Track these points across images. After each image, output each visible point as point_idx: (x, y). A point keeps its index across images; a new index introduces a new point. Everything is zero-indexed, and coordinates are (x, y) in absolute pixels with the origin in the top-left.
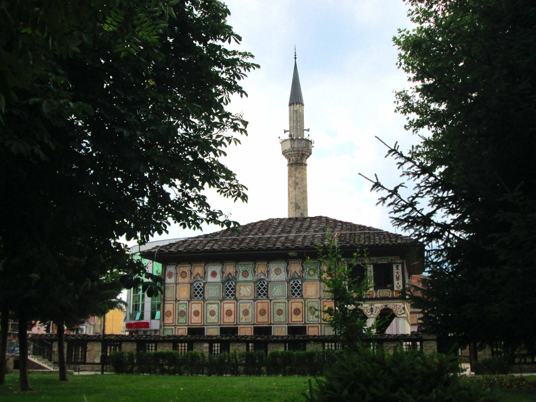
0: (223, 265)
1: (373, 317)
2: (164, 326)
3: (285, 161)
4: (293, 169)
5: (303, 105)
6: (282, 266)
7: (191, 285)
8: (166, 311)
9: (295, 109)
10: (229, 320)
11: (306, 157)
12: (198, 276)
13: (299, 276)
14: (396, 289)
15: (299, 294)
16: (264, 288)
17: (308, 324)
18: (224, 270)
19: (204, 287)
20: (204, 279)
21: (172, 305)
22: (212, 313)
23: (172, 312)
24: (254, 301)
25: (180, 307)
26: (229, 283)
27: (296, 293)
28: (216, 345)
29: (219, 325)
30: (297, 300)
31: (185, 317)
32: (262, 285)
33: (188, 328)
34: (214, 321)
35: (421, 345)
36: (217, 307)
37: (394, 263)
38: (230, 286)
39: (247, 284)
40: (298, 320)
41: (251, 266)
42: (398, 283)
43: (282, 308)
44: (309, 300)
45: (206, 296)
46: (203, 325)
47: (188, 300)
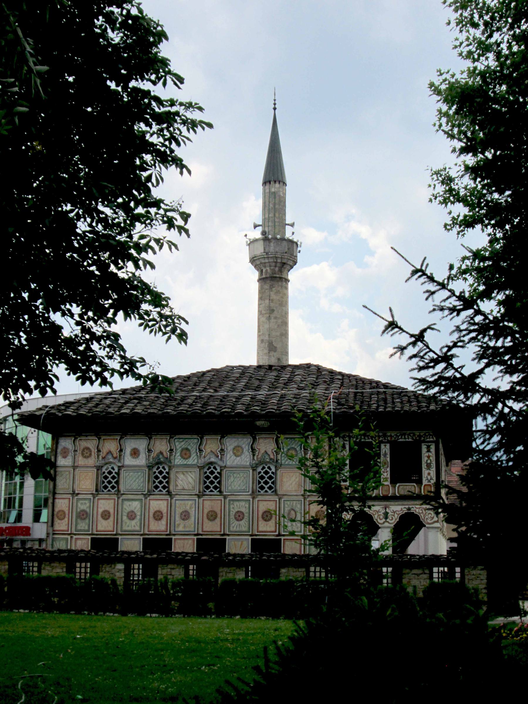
0: (150, 438)
1: (388, 527)
2: (54, 534)
3: (256, 275)
4: (267, 286)
5: (285, 184)
6: (245, 442)
7: (98, 470)
8: (56, 510)
9: (273, 190)
10: (158, 528)
11: (288, 267)
12: (110, 456)
13: (271, 459)
14: (425, 482)
15: (270, 488)
16: (216, 478)
17: (284, 535)
18: (151, 447)
19: (118, 474)
20: (119, 461)
21: (66, 501)
22: (131, 516)
23: (67, 512)
24: (199, 496)
25: (79, 504)
26: (159, 468)
27: (266, 487)
28: (136, 566)
29: (141, 535)
30: (267, 498)
31: (87, 521)
32: (212, 473)
34: (133, 528)
35: (462, 573)
36: (139, 506)
37: (424, 441)
38: (161, 473)
39: (187, 470)
40: (269, 529)
41: (196, 441)
42: (429, 474)
43: (243, 510)
44: (285, 498)
45: (122, 488)
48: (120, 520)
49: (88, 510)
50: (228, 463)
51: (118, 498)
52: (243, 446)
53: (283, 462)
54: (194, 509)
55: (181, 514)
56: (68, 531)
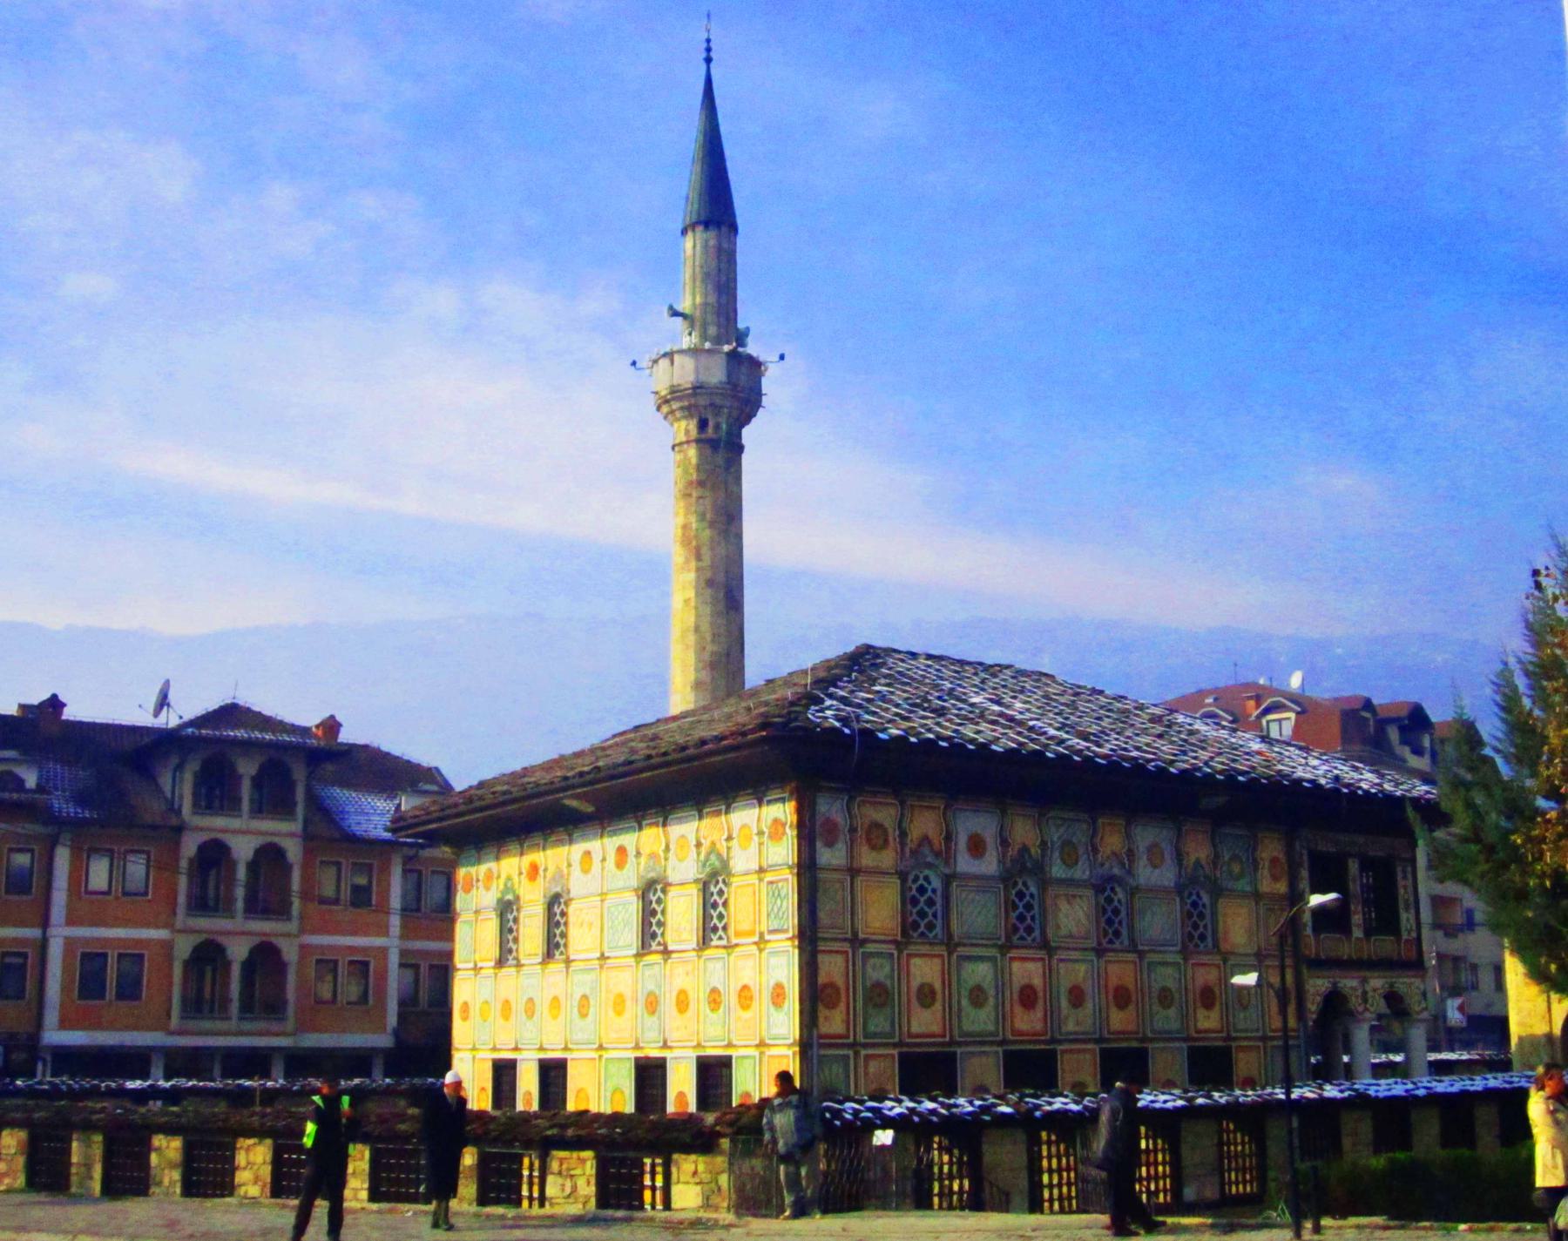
0: (1004, 812)
12: (926, 850)
13: (1206, 877)
14: (1405, 936)
17: (1235, 1039)
20: (947, 863)
21: (840, 959)
24: (1100, 952)
25: (869, 970)
31: (888, 1010)
33: (901, 1054)
34: (982, 1026)
36: (990, 977)
39: (1072, 891)
41: (1085, 826)
43: (1170, 984)
46: (952, 1043)
47: (895, 942)
48: (955, 1008)
49: (888, 983)
50: (1142, 881)
51: (950, 954)
52: (1163, 845)
56: (847, 1037)
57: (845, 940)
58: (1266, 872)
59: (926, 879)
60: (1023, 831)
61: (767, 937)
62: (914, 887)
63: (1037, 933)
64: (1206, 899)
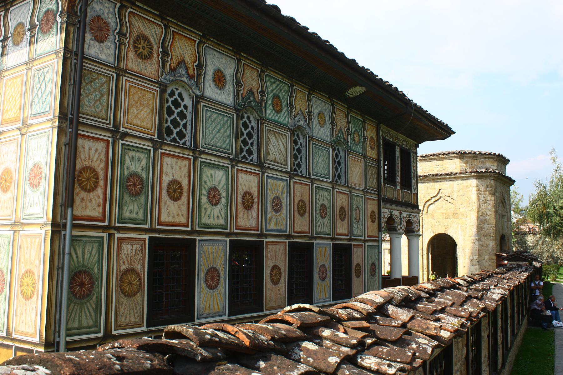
0: (239, 61)
7: (163, 91)
12: (183, 72)
13: (344, 139)
20: (197, 86)
21: (101, 146)
23: (101, 174)
25: (128, 161)
31: (142, 199)
34: (216, 222)
36: (223, 181)
39: (277, 130)
43: (326, 203)
46: (192, 232)
47: (151, 140)
49: (144, 175)
51: (195, 159)
52: (326, 113)
53: (351, 145)
54: (285, 195)
55: (273, 203)
56: (104, 221)
57: (107, 130)
58: (368, 143)
59: (180, 95)
60: (251, 80)
61: (30, 122)
62: (171, 100)
63: (255, 155)
64: (342, 154)
